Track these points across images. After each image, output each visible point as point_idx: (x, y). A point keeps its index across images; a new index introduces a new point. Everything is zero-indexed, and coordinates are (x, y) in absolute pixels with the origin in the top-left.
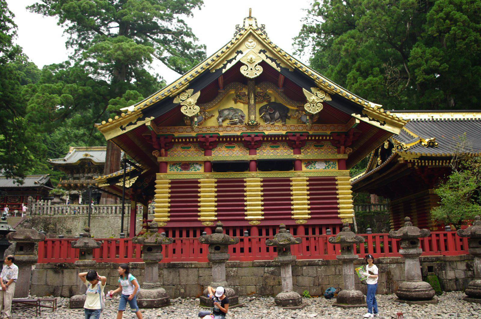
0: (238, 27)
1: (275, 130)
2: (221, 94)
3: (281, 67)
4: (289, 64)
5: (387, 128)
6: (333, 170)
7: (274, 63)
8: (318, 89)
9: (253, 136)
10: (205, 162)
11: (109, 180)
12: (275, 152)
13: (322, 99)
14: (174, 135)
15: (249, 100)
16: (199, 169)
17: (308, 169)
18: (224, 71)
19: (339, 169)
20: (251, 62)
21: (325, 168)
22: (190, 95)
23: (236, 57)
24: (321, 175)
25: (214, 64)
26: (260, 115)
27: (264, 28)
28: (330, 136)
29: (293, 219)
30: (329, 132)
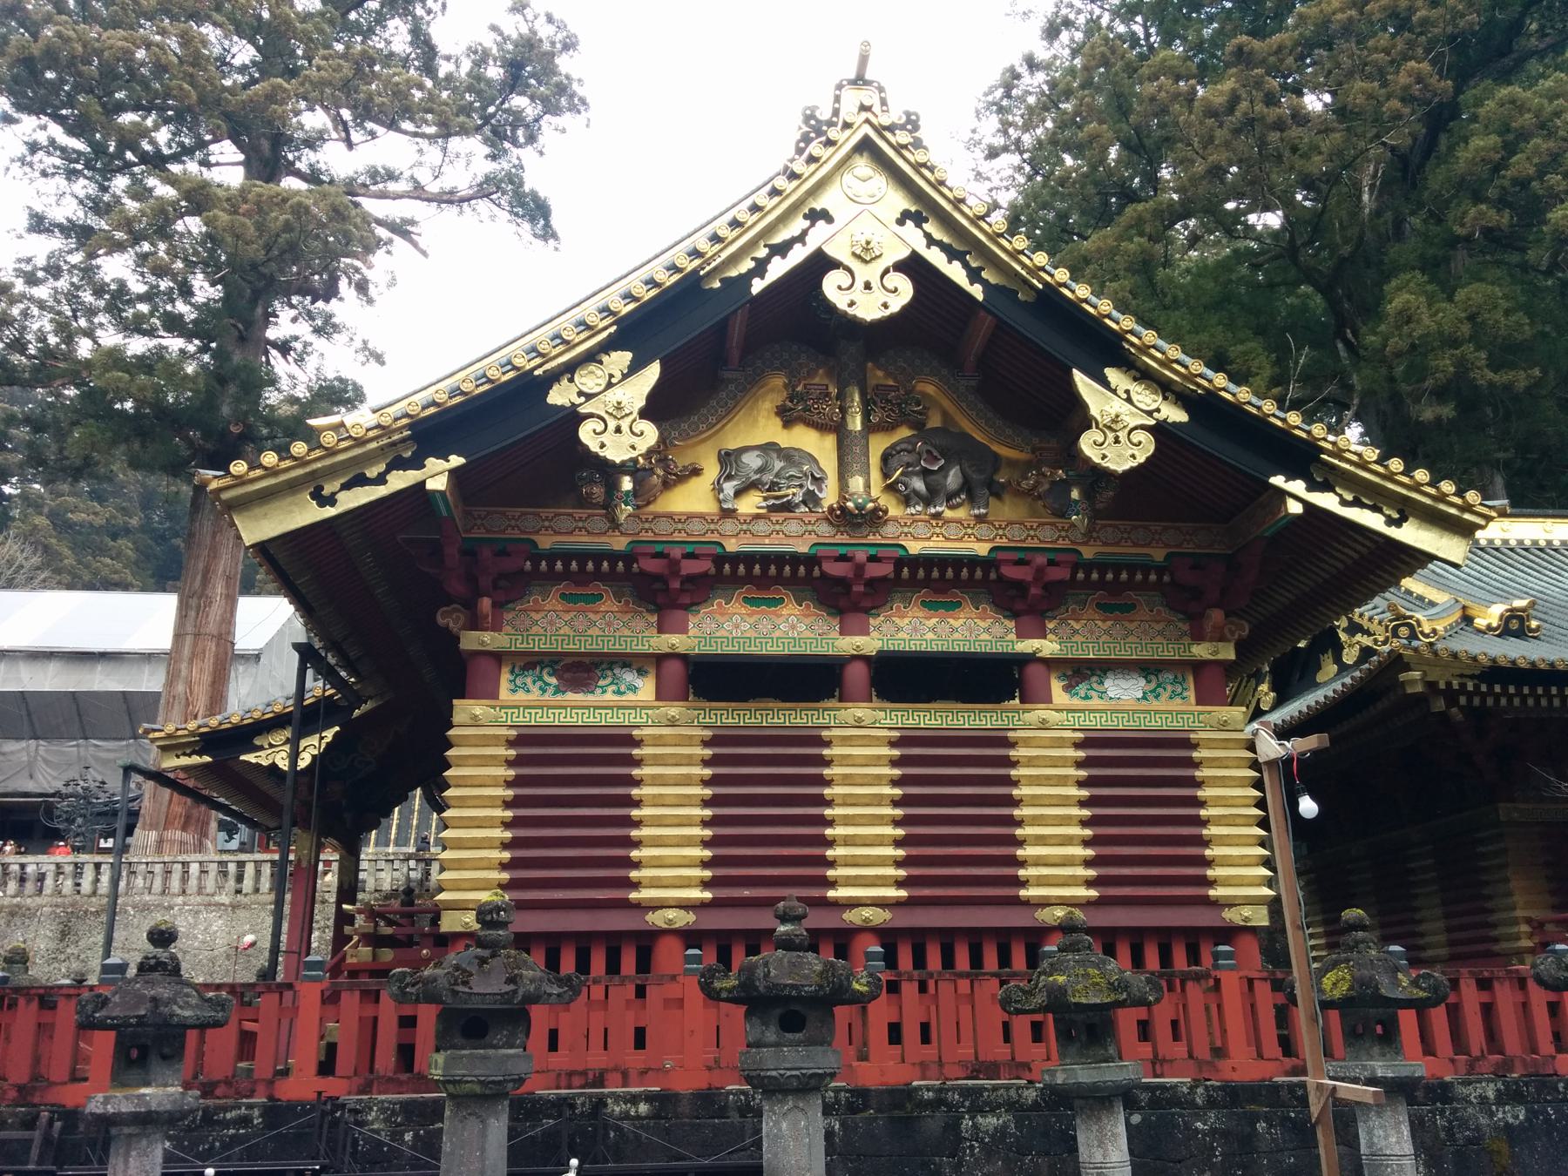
0: (812, 116)
1: (947, 539)
2: (732, 387)
3: (984, 283)
4: (1018, 268)
5: (1412, 534)
6: (1177, 704)
7: (957, 264)
8: (1133, 372)
9: (861, 556)
10: (659, 659)
11: (211, 741)
12: (944, 629)
13: (1150, 413)
14: (534, 544)
15: (844, 418)
16: (634, 689)
17: (1076, 702)
18: (757, 286)
19: (1199, 703)
20: (865, 255)
21: (1144, 698)
22: (618, 376)
23: (805, 233)
24: (1132, 725)
25: (717, 254)
26: (886, 476)
27: (916, 128)
28: (1160, 570)
29: (1027, 903)
30: (1159, 555)
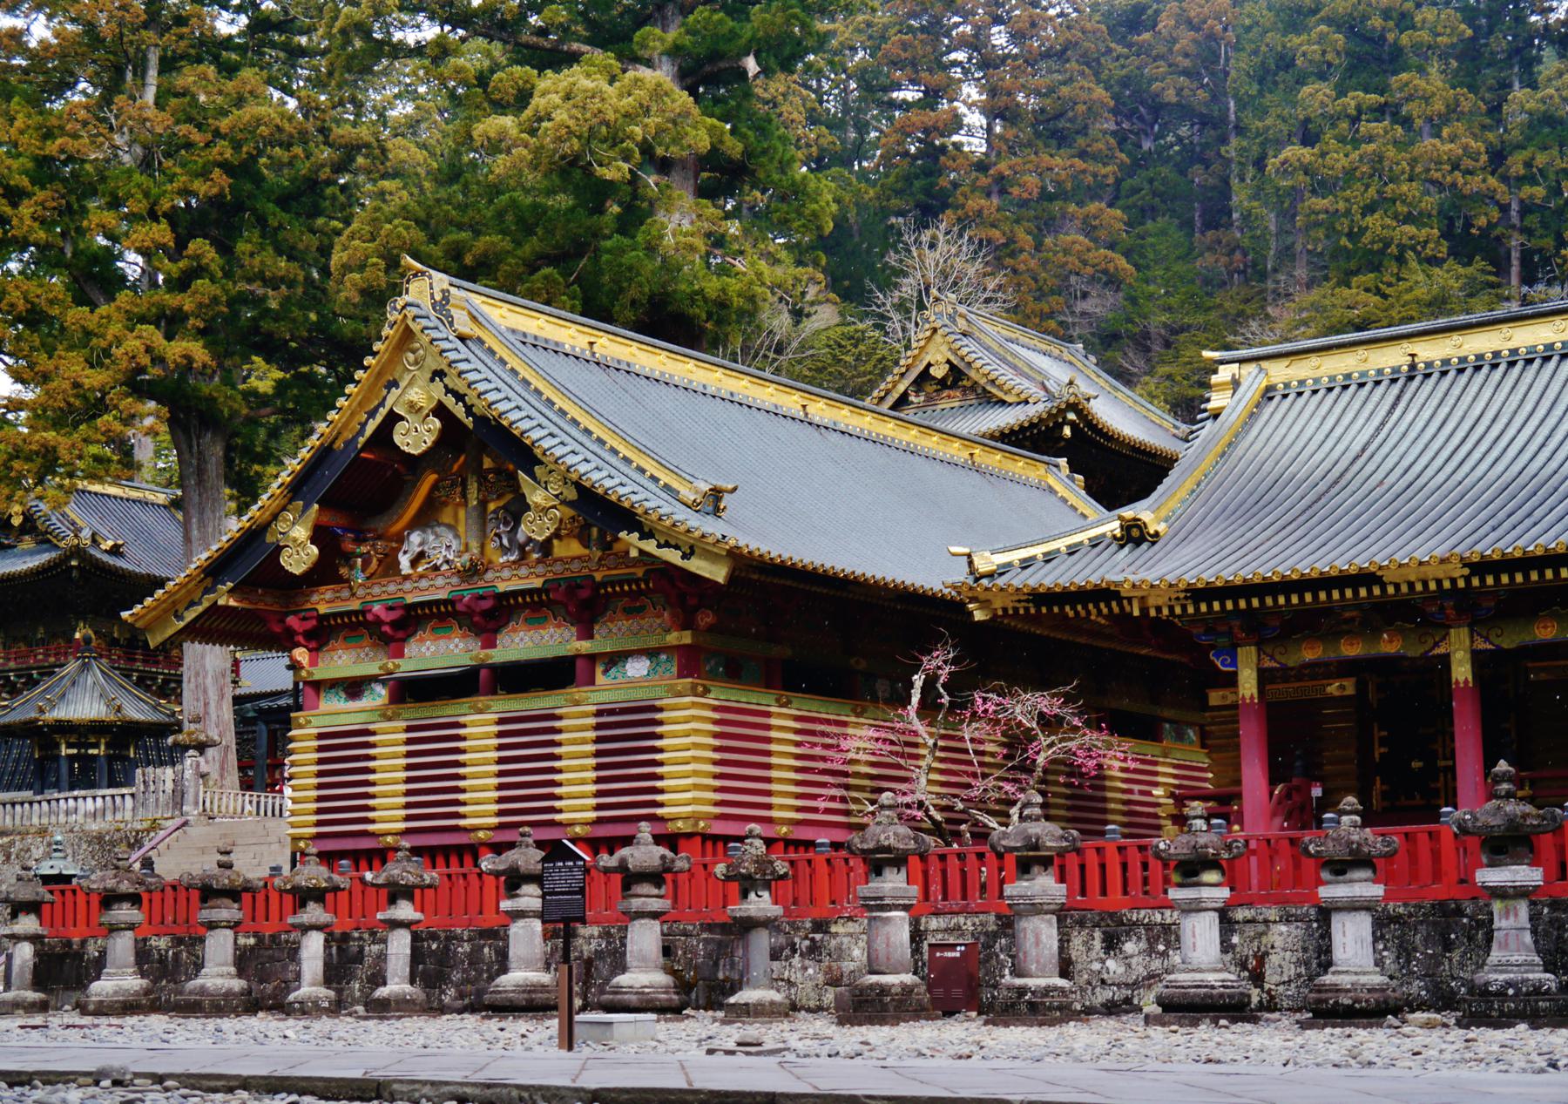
12: (536, 637)
18: (362, 440)
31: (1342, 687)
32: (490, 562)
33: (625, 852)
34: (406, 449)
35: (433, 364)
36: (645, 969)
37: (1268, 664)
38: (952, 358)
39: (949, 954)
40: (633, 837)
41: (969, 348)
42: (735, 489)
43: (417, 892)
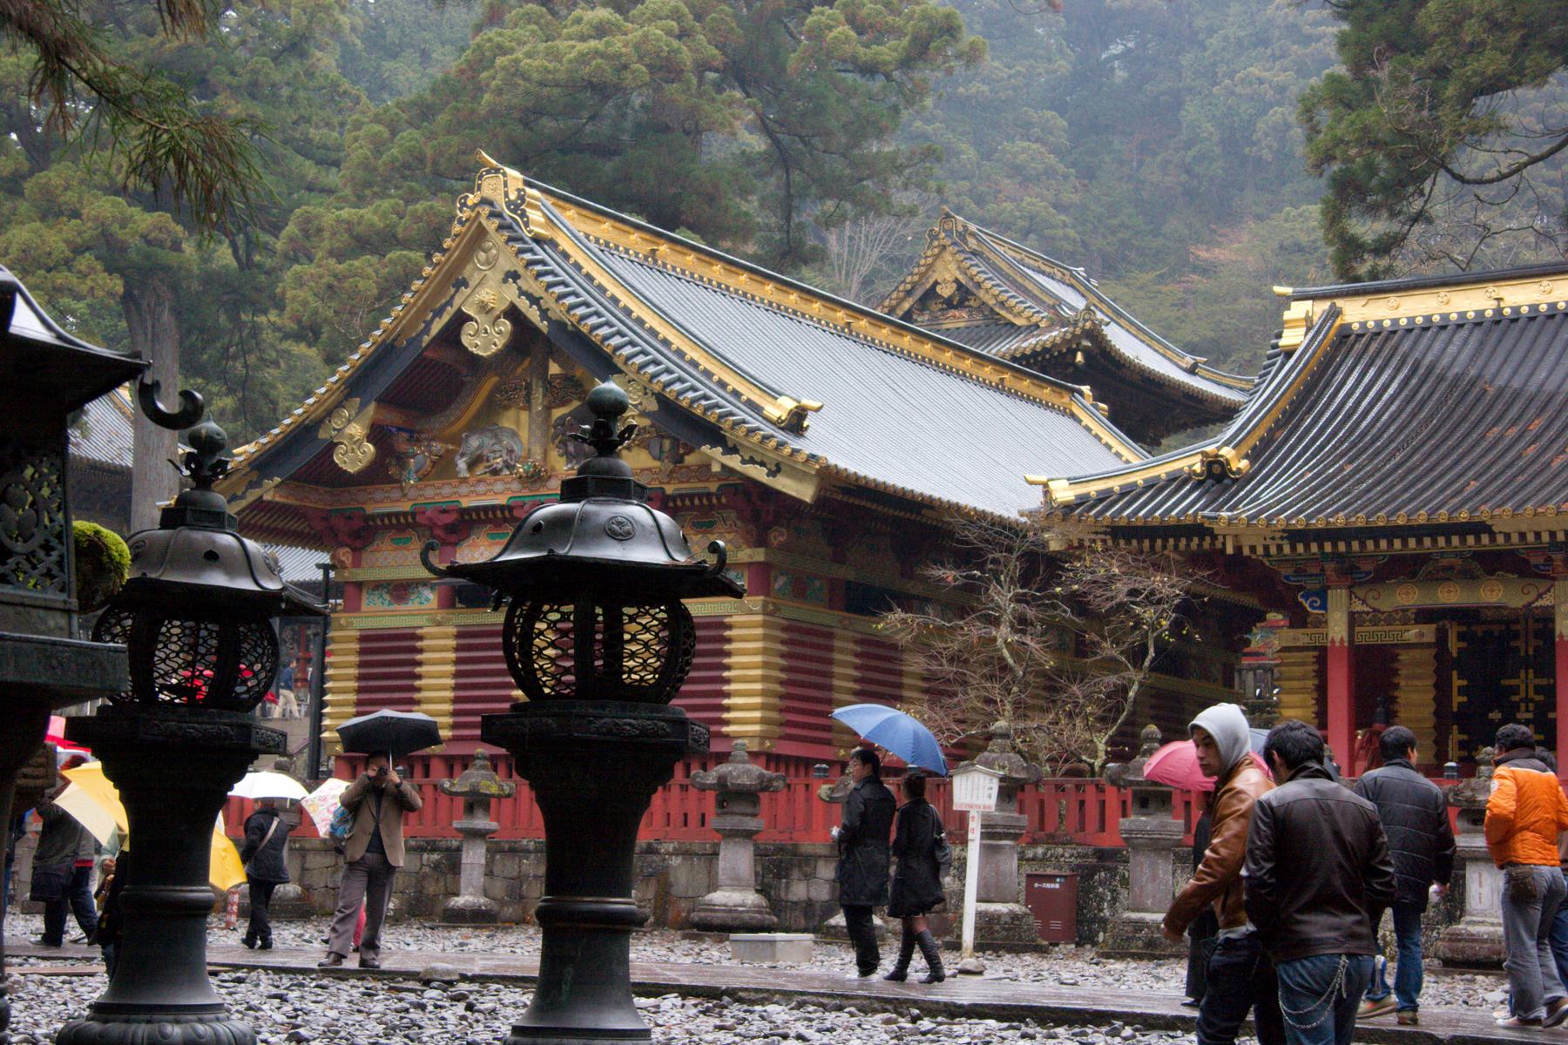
3: (549, 320)
18: (426, 339)
31: (1421, 635)
32: (553, 469)
33: (724, 768)
34: (475, 351)
35: (507, 262)
36: (737, 884)
37: (1358, 607)
38: (961, 278)
39: (1048, 886)
40: (729, 754)
41: (978, 270)
42: (821, 408)
43: (493, 802)
